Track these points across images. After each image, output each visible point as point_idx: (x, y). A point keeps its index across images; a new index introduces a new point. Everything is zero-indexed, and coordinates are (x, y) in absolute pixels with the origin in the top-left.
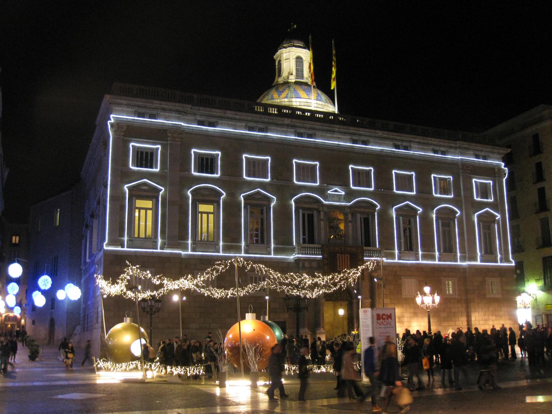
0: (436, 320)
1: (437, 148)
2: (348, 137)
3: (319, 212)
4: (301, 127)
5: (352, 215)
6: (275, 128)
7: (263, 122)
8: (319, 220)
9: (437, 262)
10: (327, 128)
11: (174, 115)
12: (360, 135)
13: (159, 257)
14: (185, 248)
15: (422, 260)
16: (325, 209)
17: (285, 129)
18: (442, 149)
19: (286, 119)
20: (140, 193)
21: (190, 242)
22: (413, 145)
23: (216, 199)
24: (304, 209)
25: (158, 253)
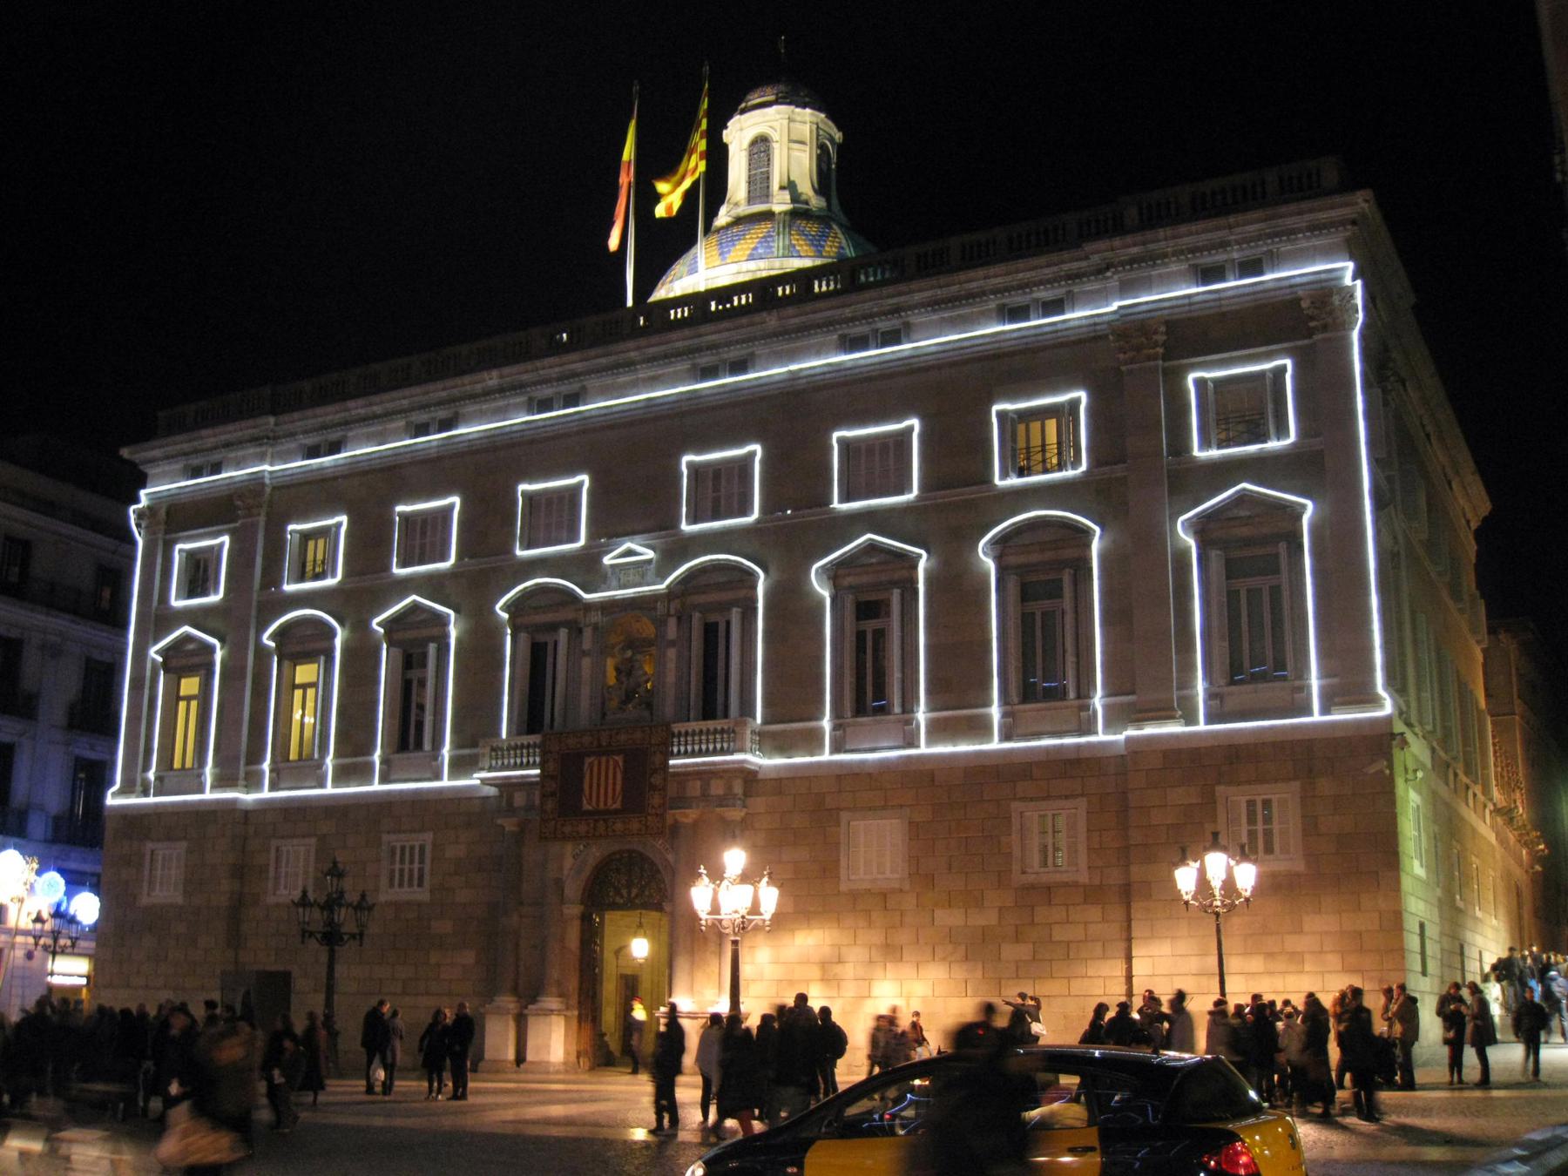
0: (979, 974)
1: (1018, 299)
2: (683, 366)
3: (576, 630)
4: (535, 384)
5: (679, 618)
6: (477, 407)
7: (440, 403)
8: (575, 651)
9: (995, 744)
10: (603, 361)
11: (251, 451)
12: (713, 347)
13: (197, 813)
14: (253, 782)
15: (929, 742)
16: (596, 617)
17: (501, 403)
18: (1044, 294)
19: (485, 375)
20: (184, 662)
21: (266, 766)
22: (916, 318)
23: (324, 644)
24: (526, 628)
25: (375, 794)
